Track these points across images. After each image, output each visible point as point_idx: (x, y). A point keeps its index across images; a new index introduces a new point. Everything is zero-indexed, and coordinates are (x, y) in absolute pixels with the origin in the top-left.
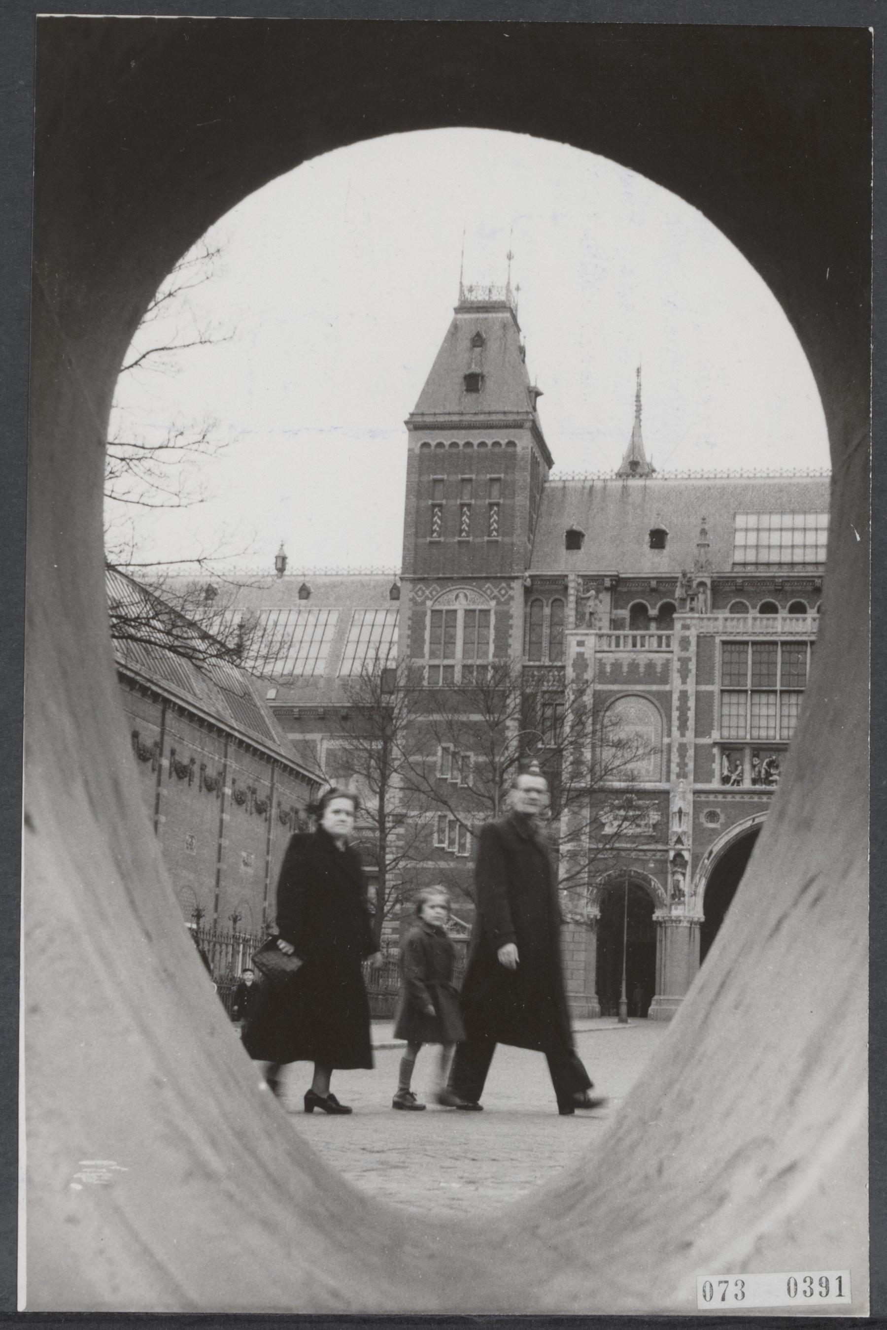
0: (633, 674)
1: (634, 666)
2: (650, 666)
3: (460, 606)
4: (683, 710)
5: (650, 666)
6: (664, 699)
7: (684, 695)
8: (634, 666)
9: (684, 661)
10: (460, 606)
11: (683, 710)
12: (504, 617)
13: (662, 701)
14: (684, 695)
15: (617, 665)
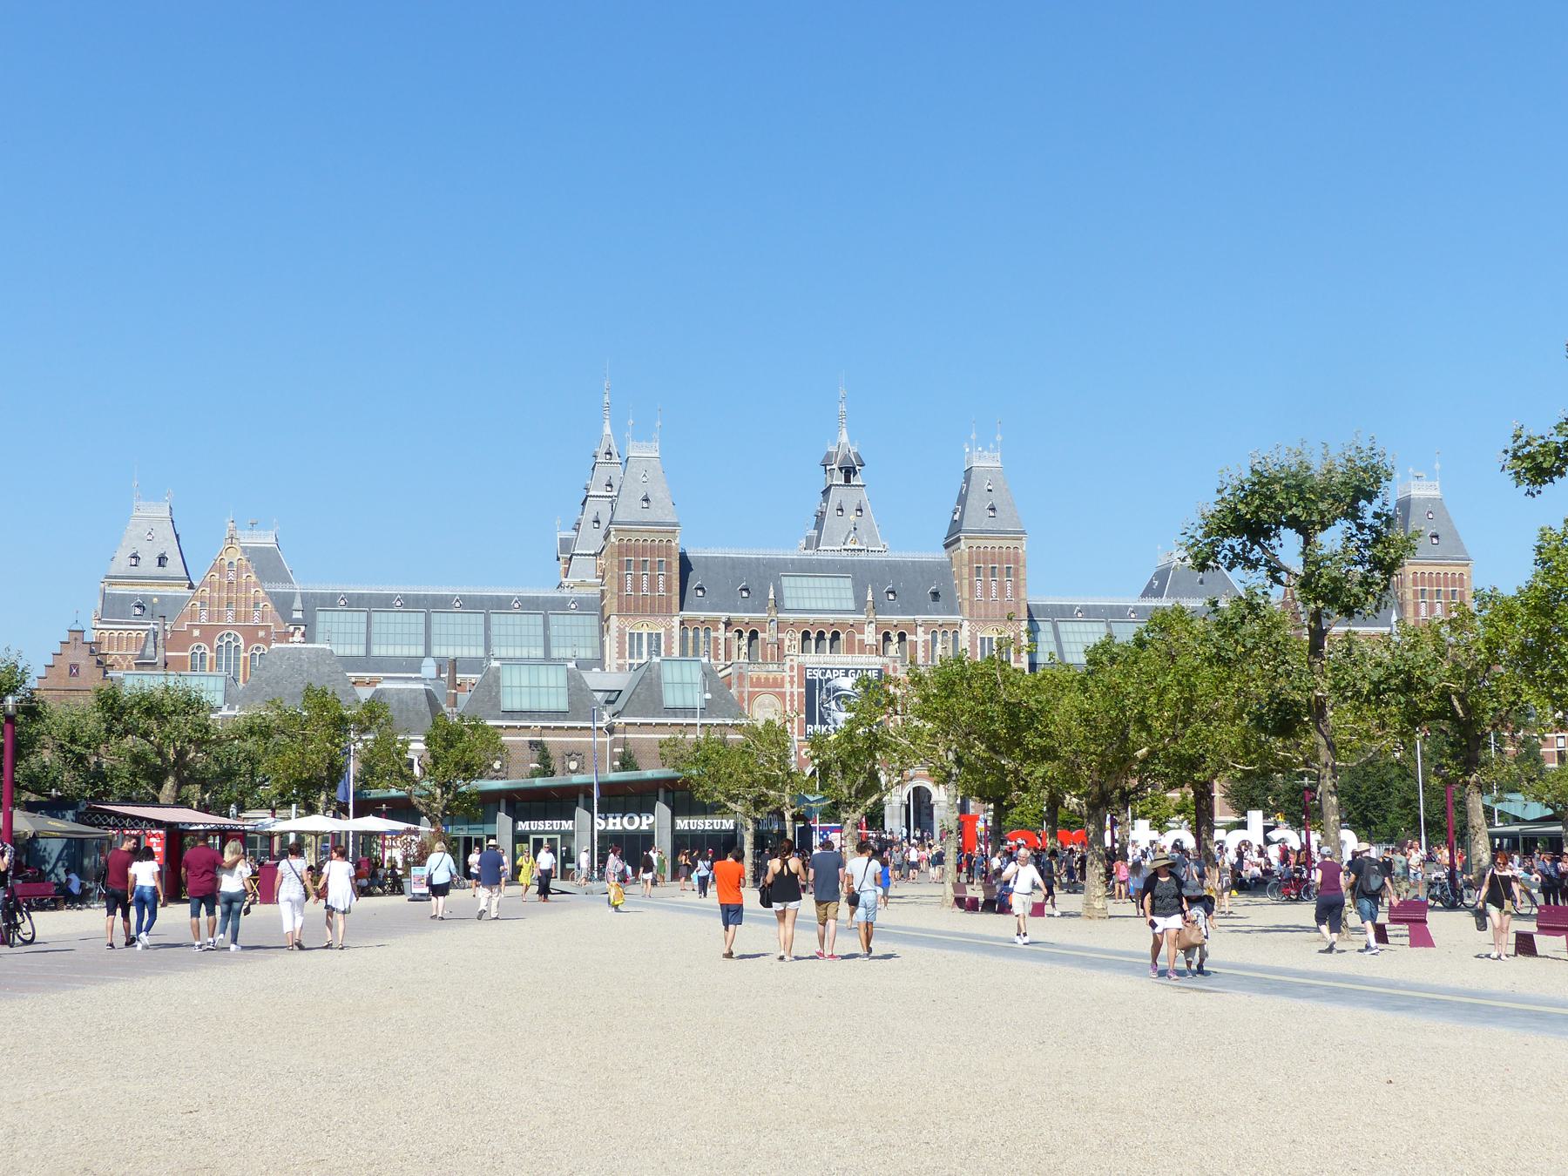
0: (767, 683)
1: (767, 679)
2: (775, 679)
3: (645, 631)
4: (792, 701)
5: (775, 679)
6: (782, 696)
7: (792, 694)
8: (767, 679)
9: (792, 677)
10: (645, 631)
11: (792, 701)
12: (669, 637)
13: (782, 696)
14: (792, 694)
15: (758, 679)
